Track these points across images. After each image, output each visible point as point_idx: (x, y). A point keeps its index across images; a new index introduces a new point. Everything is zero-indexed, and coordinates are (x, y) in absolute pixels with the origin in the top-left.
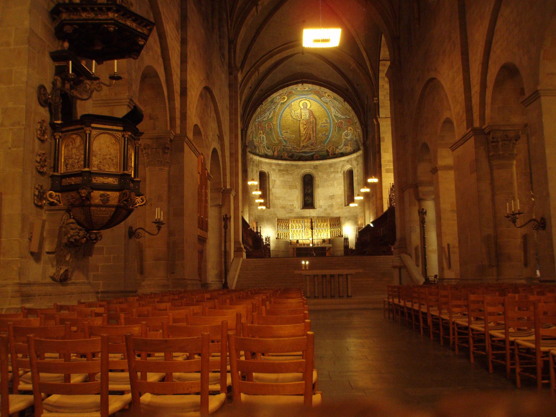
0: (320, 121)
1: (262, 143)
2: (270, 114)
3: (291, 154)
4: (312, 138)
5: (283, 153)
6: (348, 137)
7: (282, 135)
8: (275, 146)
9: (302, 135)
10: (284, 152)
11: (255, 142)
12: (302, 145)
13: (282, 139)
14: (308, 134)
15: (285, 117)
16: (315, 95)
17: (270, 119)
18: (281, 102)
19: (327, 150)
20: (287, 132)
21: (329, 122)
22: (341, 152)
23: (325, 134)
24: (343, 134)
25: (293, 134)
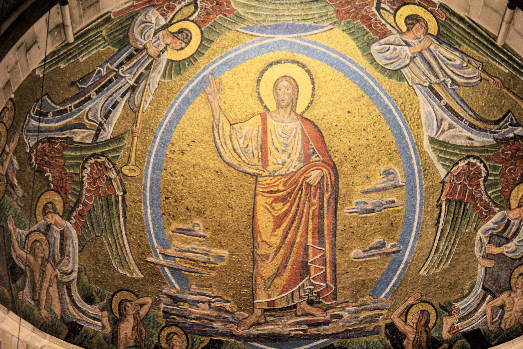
0: (357, 180)
1: (56, 265)
2: (107, 116)
3: (206, 340)
4: (312, 267)
5: (164, 334)
6: (512, 245)
7: (165, 244)
8: (126, 295)
9: (262, 250)
10: (173, 329)
11: (16, 245)
12: (262, 299)
13: (161, 260)
14: (294, 249)
15: (183, 152)
16: (337, 31)
17: (108, 142)
18: (171, 55)
19: (391, 327)
20: (188, 232)
21: (401, 180)
22: (466, 326)
23: (383, 245)
24: (479, 233)
25: (220, 245)
